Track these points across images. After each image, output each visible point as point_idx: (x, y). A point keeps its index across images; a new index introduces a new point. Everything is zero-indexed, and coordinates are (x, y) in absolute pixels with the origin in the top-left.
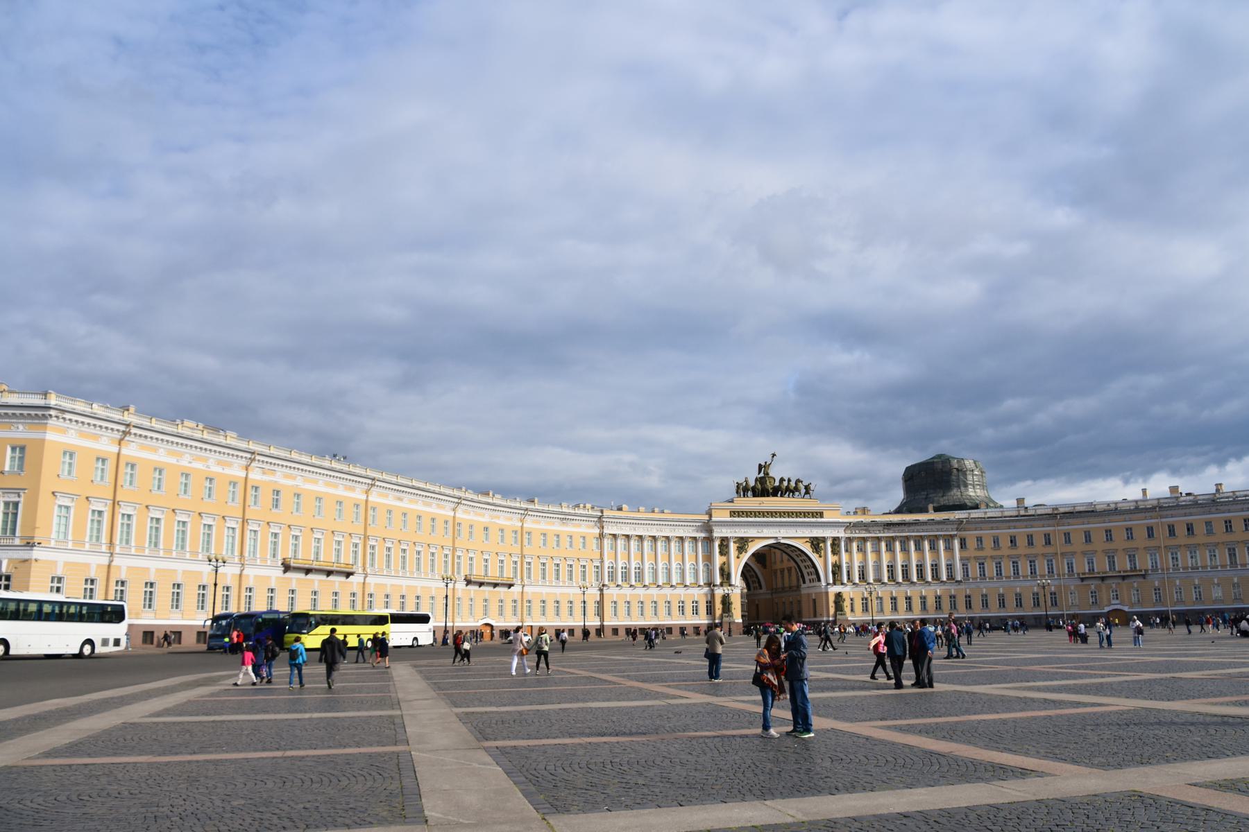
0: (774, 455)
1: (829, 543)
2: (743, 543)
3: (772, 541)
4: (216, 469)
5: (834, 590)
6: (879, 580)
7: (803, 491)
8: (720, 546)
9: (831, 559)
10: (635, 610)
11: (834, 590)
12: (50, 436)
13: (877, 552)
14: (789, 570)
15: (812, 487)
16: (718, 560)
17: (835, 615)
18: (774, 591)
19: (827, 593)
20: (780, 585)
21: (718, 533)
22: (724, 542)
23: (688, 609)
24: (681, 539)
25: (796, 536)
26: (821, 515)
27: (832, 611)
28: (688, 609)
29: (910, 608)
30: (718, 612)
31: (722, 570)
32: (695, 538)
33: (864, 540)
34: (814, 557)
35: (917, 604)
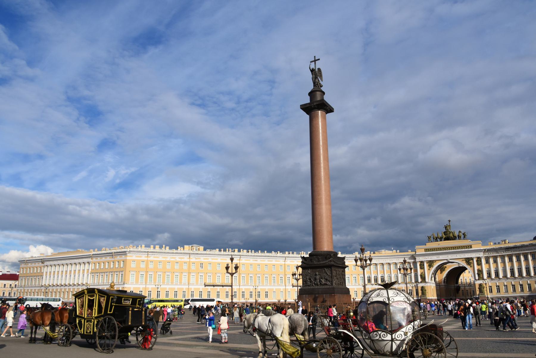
2: (431, 263)
3: (446, 261)
4: (178, 260)
6: (505, 276)
7: (462, 236)
8: (420, 265)
12: (128, 258)
13: (504, 262)
15: (466, 234)
16: (419, 271)
17: (479, 295)
19: (475, 284)
21: (418, 259)
26: (471, 247)
27: (478, 292)
29: (522, 290)
30: (420, 294)
31: (421, 276)
35: (526, 288)
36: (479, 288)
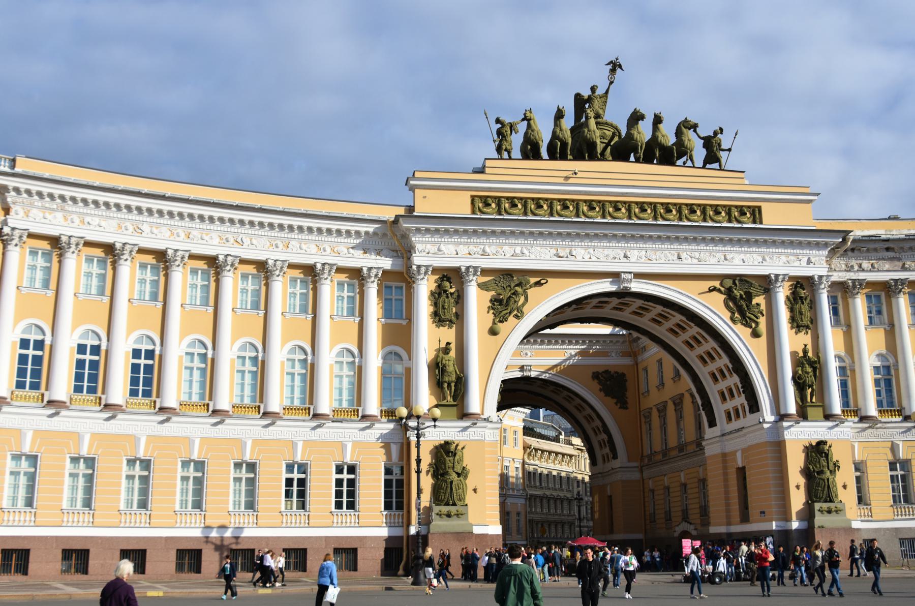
0: (615, 66)
1: (782, 293)
2: (508, 290)
5: (799, 436)
7: (699, 153)
8: (437, 295)
9: (791, 342)
10: (171, 489)
11: (799, 436)
14: (678, 402)
15: (725, 141)
16: (428, 338)
17: (808, 514)
18: (645, 461)
20: (658, 446)
21: (430, 253)
22: (450, 282)
23: (322, 489)
24: (311, 273)
25: (681, 270)
27: (798, 500)
28: (322, 489)
31: (437, 368)
32: (357, 275)
33: (888, 289)
34: (737, 335)
36: (807, 473)
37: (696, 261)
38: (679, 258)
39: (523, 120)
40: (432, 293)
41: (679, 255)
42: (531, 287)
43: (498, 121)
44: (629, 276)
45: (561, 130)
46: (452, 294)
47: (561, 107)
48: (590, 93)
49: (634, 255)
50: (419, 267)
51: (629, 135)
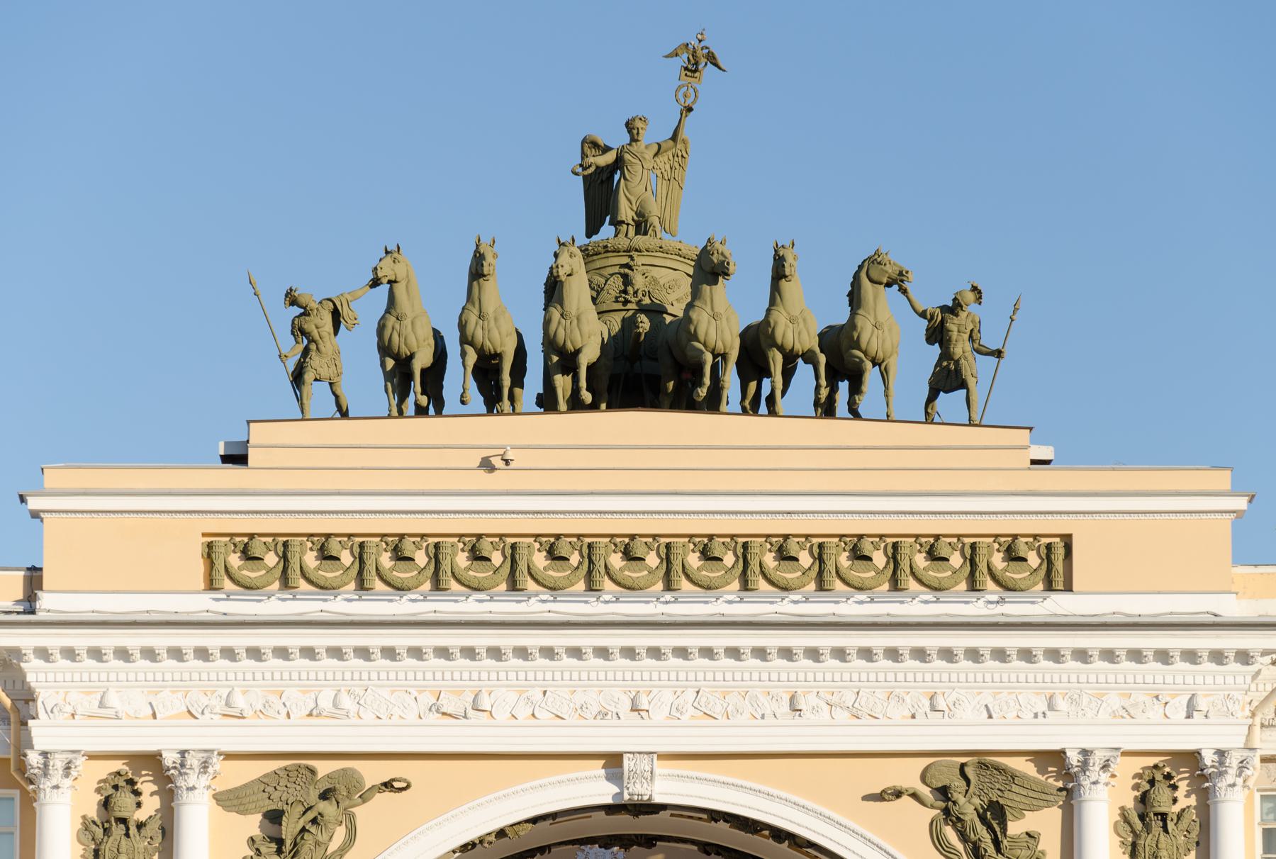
0: (697, 61)
15: (989, 319)
37: (842, 716)
38: (795, 709)
39: (375, 283)
40: (87, 824)
41: (792, 699)
42: (364, 799)
43: (292, 299)
44: (644, 764)
45: (481, 316)
46: (140, 826)
47: (486, 240)
48: (627, 139)
49: (660, 703)
50: (45, 754)
51: (687, 319)
